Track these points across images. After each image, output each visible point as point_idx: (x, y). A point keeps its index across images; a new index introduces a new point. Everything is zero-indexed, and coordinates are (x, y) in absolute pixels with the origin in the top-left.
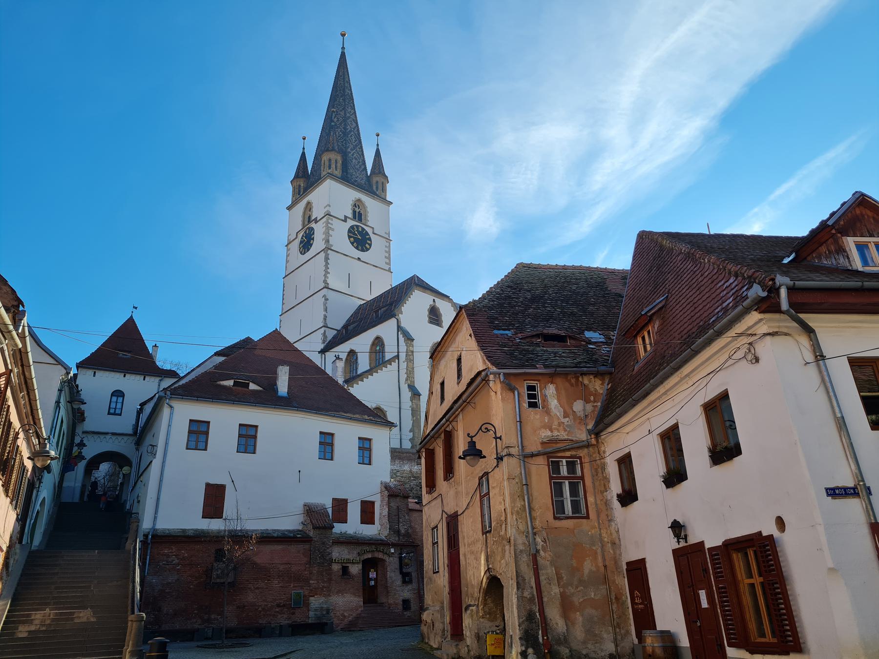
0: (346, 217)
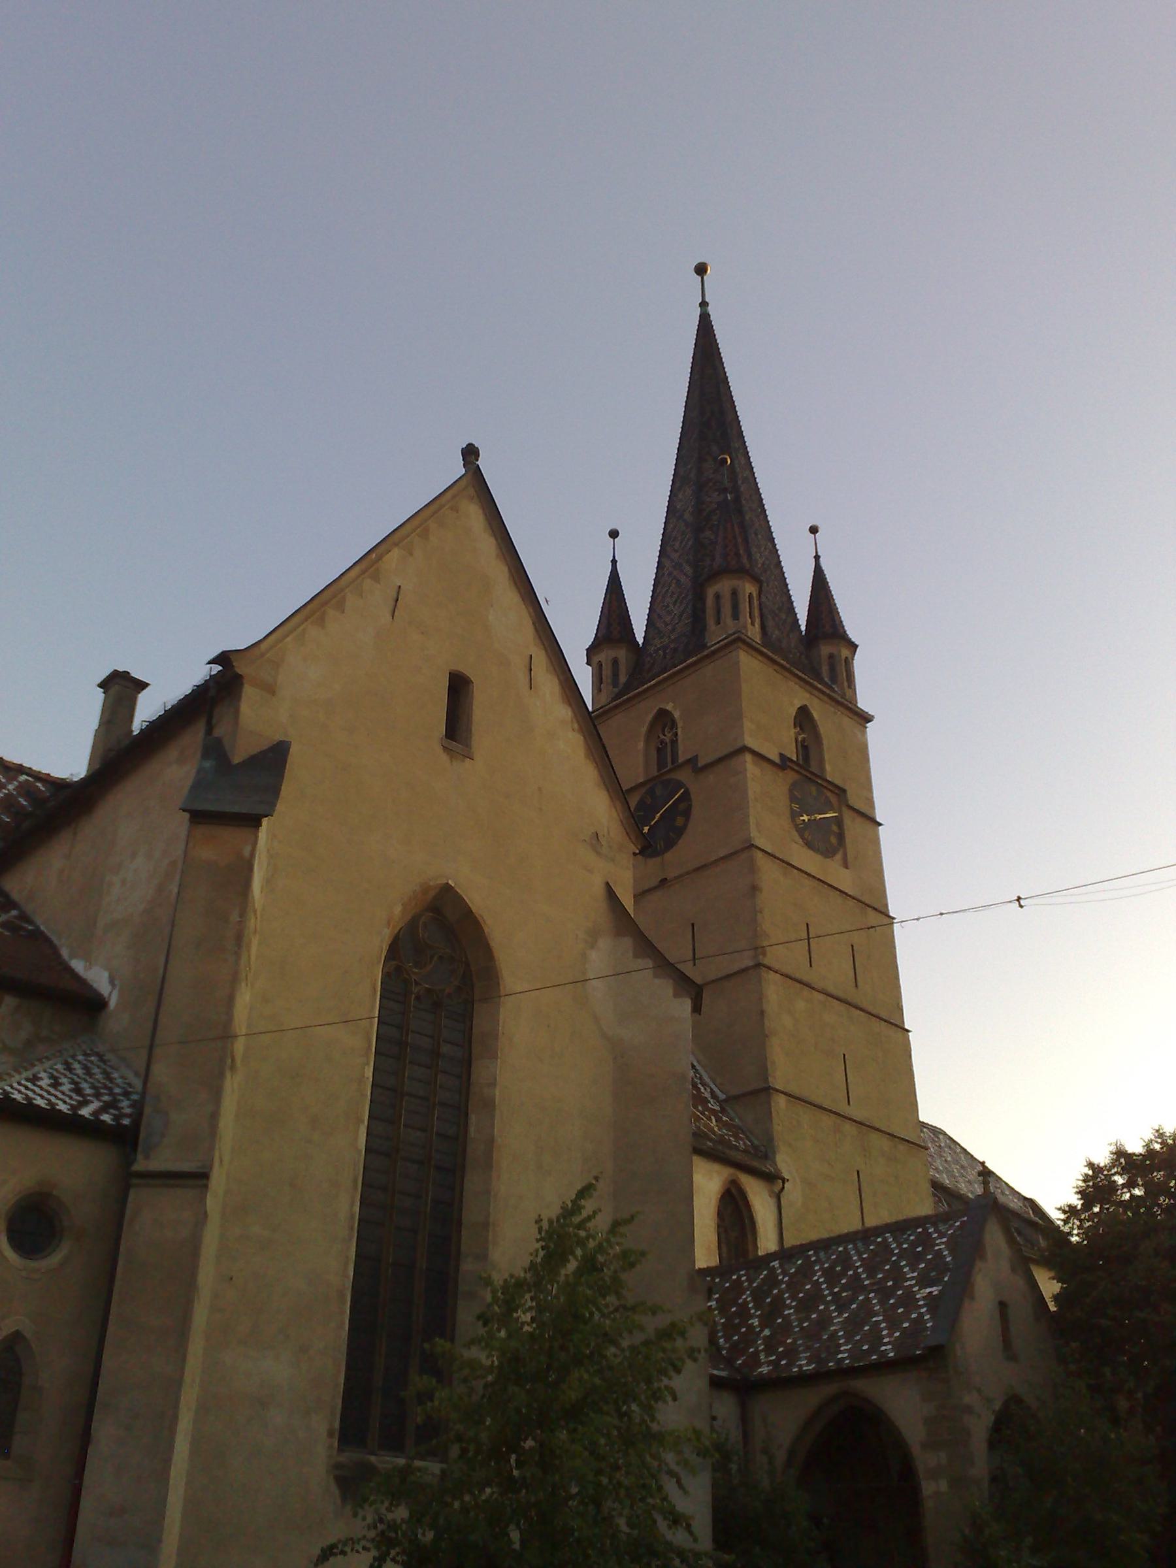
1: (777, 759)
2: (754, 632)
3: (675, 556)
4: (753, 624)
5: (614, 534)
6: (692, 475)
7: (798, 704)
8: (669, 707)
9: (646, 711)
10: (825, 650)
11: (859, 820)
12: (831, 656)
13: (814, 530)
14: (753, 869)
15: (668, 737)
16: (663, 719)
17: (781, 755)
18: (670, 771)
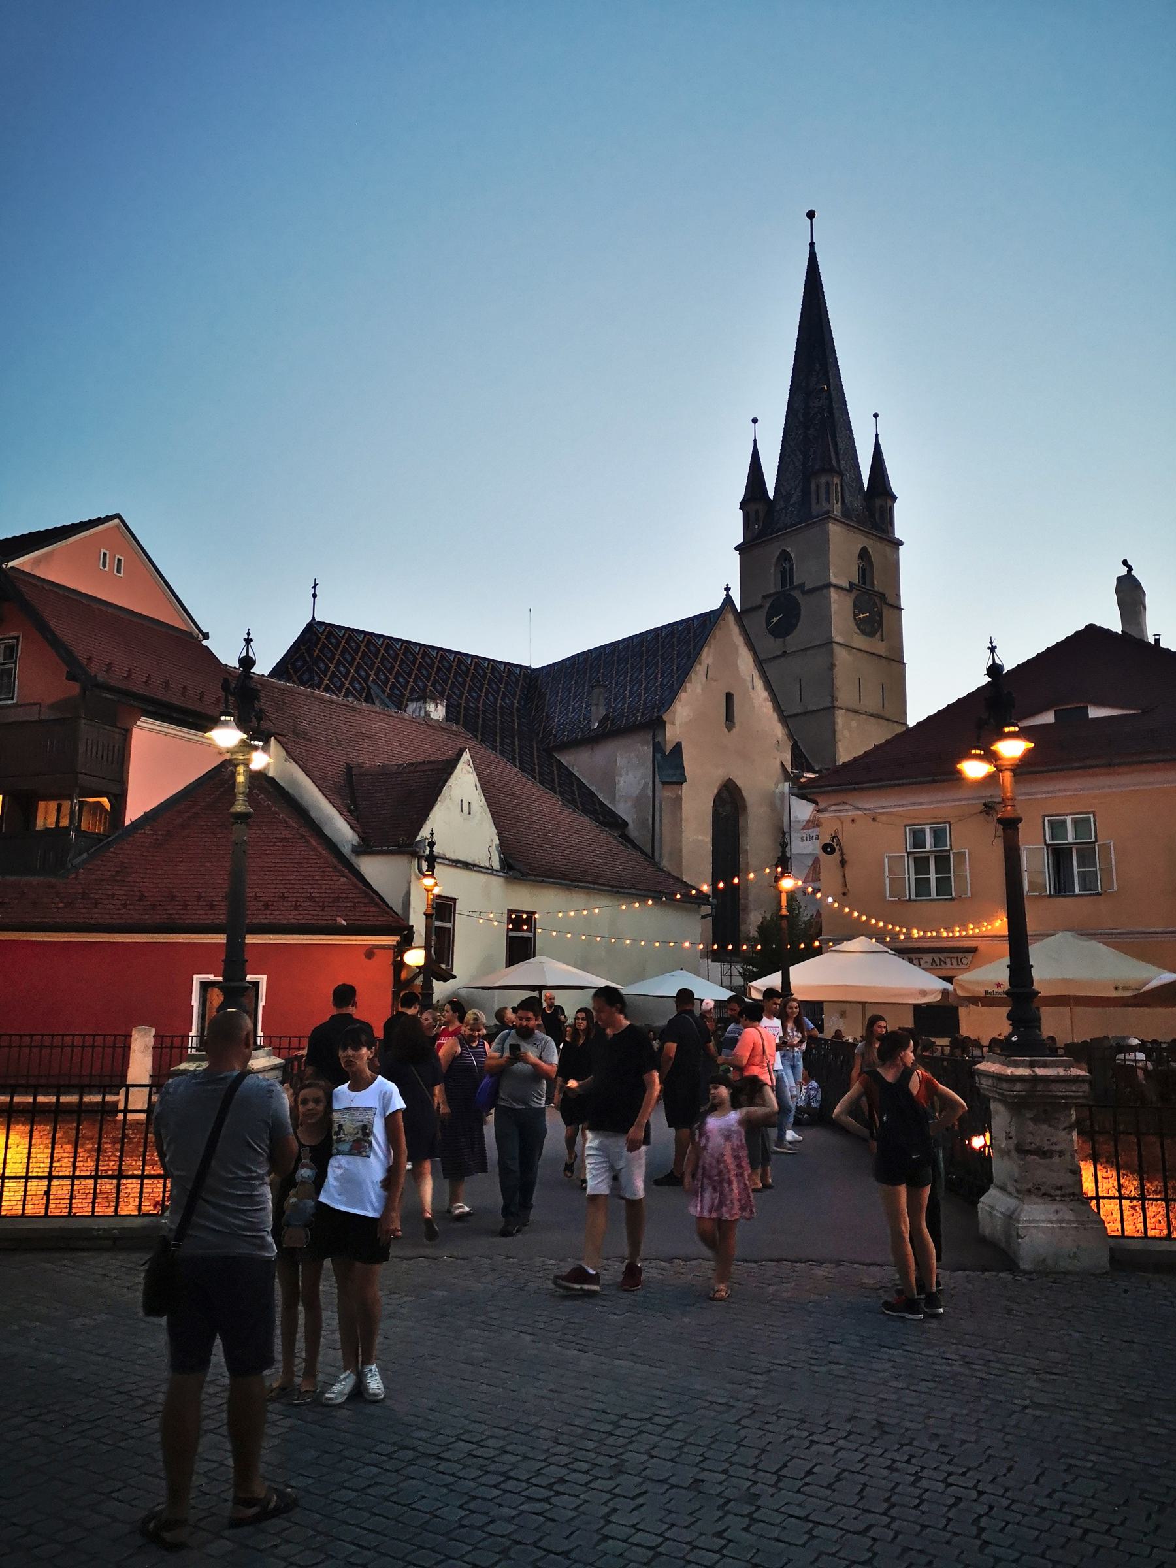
0: (764, 597)
1: (846, 585)
2: (837, 509)
3: (793, 444)
4: (837, 503)
5: (755, 421)
6: (804, 384)
7: (860, 547)
8: (789, 550)
9: (774, 551)
10: (878, 502)
11: (891, 610)
12: (881, 506)
13: (876, 416)
14: (831, 653)
15: (787, 566)
16: (785, 556)
17: (850, 583)
18: (788, 590)
